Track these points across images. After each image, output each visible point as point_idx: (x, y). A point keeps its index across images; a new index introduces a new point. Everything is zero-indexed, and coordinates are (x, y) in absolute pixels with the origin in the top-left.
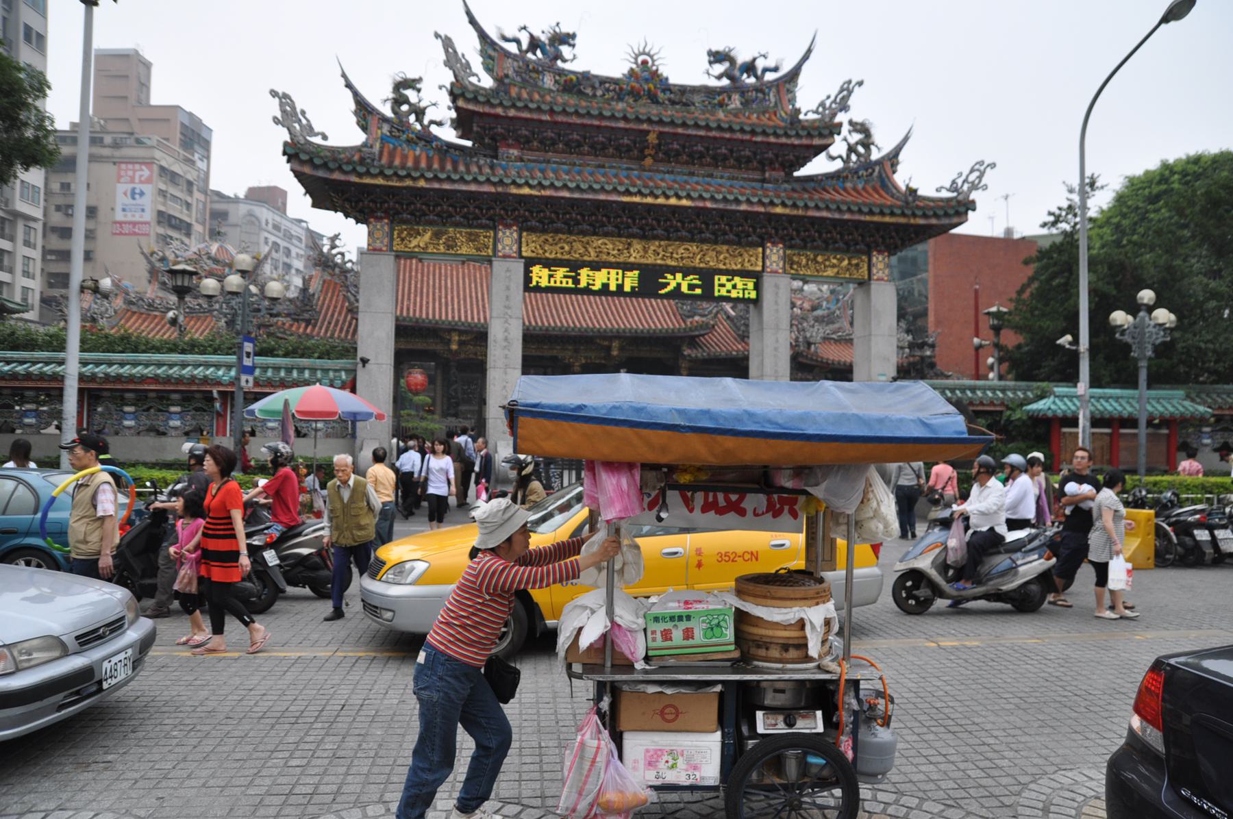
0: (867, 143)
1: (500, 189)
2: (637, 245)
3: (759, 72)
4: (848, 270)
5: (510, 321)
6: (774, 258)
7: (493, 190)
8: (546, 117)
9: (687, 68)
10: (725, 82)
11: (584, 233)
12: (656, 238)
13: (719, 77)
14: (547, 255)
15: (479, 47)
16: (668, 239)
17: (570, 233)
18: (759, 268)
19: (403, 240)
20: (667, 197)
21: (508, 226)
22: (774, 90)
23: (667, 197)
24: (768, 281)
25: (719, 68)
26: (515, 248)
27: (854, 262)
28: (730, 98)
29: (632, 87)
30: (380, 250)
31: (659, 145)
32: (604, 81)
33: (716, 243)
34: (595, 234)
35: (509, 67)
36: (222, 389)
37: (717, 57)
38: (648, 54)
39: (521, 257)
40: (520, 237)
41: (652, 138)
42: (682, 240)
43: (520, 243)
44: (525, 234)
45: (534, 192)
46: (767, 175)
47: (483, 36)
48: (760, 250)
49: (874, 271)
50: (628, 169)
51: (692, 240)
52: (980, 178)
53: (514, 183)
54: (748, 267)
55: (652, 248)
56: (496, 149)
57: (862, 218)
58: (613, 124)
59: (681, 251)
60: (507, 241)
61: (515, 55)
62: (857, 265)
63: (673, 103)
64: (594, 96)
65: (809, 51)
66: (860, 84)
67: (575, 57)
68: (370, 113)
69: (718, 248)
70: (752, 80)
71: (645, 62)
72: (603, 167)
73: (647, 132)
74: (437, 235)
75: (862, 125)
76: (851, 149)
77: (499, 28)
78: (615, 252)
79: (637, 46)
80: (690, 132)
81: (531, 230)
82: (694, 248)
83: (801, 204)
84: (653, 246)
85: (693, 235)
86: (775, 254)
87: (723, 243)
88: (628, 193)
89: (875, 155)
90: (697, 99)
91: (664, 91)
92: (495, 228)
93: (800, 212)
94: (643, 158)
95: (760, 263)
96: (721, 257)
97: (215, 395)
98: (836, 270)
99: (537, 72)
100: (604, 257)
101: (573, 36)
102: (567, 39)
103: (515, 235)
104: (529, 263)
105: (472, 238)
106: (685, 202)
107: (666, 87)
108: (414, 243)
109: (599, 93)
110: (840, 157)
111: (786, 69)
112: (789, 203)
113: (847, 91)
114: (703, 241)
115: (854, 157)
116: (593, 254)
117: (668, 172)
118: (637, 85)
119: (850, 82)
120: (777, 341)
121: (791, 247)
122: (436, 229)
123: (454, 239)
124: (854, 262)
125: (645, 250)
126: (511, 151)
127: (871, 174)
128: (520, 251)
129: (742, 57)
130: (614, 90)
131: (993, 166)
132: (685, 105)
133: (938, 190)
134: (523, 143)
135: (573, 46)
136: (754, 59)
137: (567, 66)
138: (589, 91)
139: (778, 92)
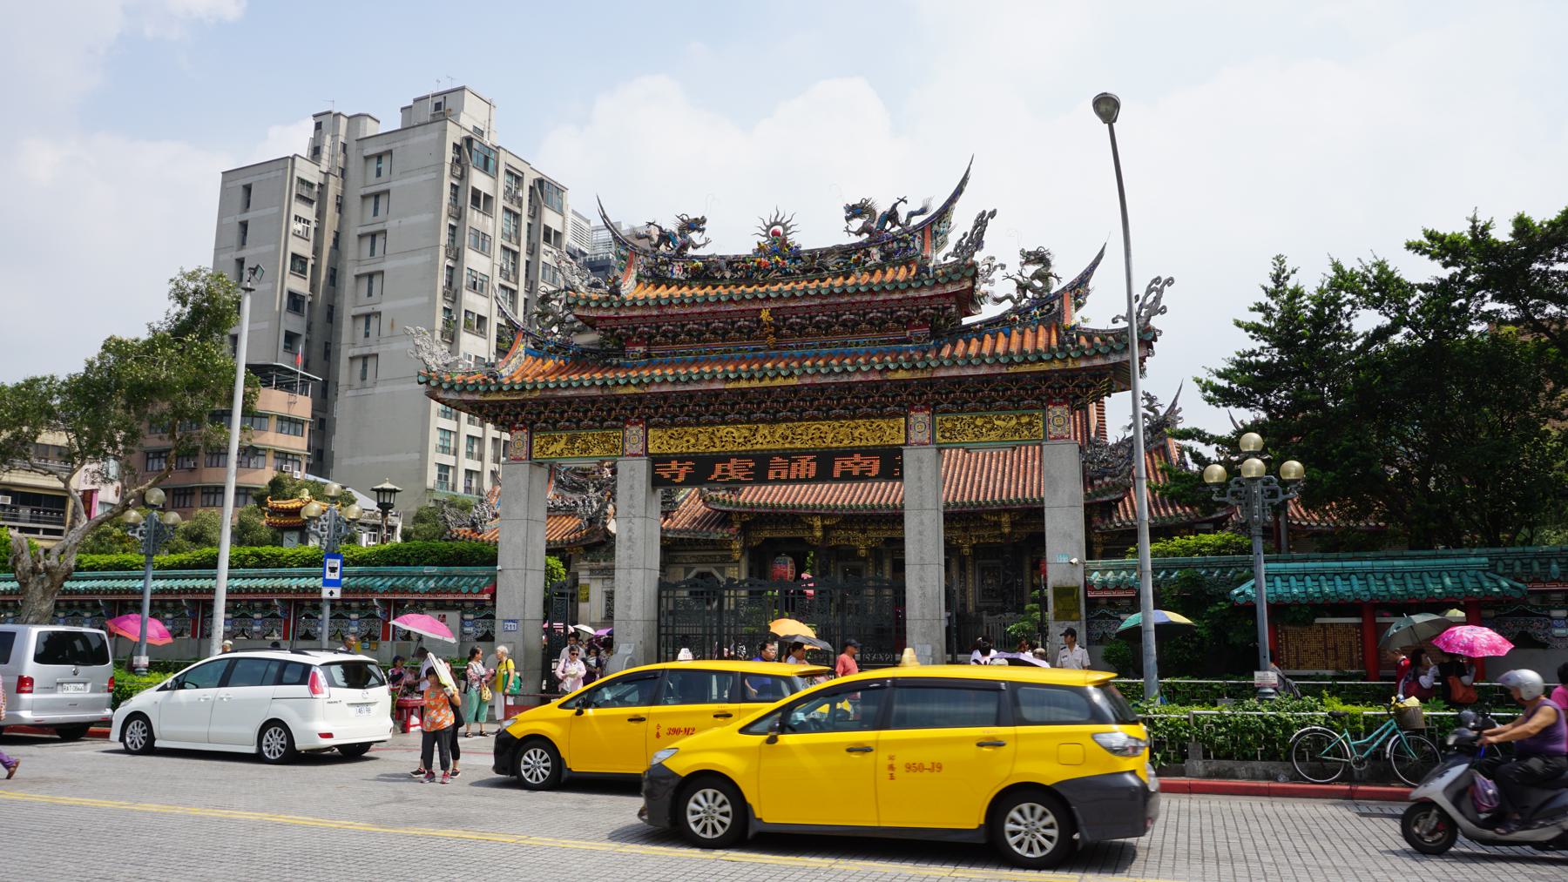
0: (1043, 277)
2: (764, 429)
3: (902, 218)
4: (1017, 431)
5: (636, 520)
9: (821, 229)
10: (866, 236)
13: (859, 233)
21: (636, 424)
24: (909, 456)
25: (857, 223)
27: (1025, 420)
28: (868, 254)
32: (731, 262)
37: (855, 211)
39: (647, 454)
42: (814, 419)
52: (1157, 300)
56: (623, 349)
59: (811, 431)
62: (1030, 423)
64: (723, 278)
66: (993, 214)
67: (707, 241)
70: (897, 228)
71: (775, 233)
74: (572, 440)
75: (1036, 253)
76: (1022, 288)
81: (658, 426)
84: (781, 429)
89: (1056, 287)
90: (831, 262)
91: (794, 261)
92: (623, 428)
100: (729, 447)
101: (703, 221)
102: (696, 225)
107: (796, 255)
109: (728, 275)
110: (1009, 297)
111: (935, 207)
113: (981, 222)
114: (838, 418)
115: (1029, 294)
117: (797, 347)
120: (922, 523)
124: (1025, 420)
125: (772, 434)
129: (882, 207)
131: (1170, 281)
133: (1114, 321)
134: (648, 340)
137: (700, 252)
138: (718, 275)
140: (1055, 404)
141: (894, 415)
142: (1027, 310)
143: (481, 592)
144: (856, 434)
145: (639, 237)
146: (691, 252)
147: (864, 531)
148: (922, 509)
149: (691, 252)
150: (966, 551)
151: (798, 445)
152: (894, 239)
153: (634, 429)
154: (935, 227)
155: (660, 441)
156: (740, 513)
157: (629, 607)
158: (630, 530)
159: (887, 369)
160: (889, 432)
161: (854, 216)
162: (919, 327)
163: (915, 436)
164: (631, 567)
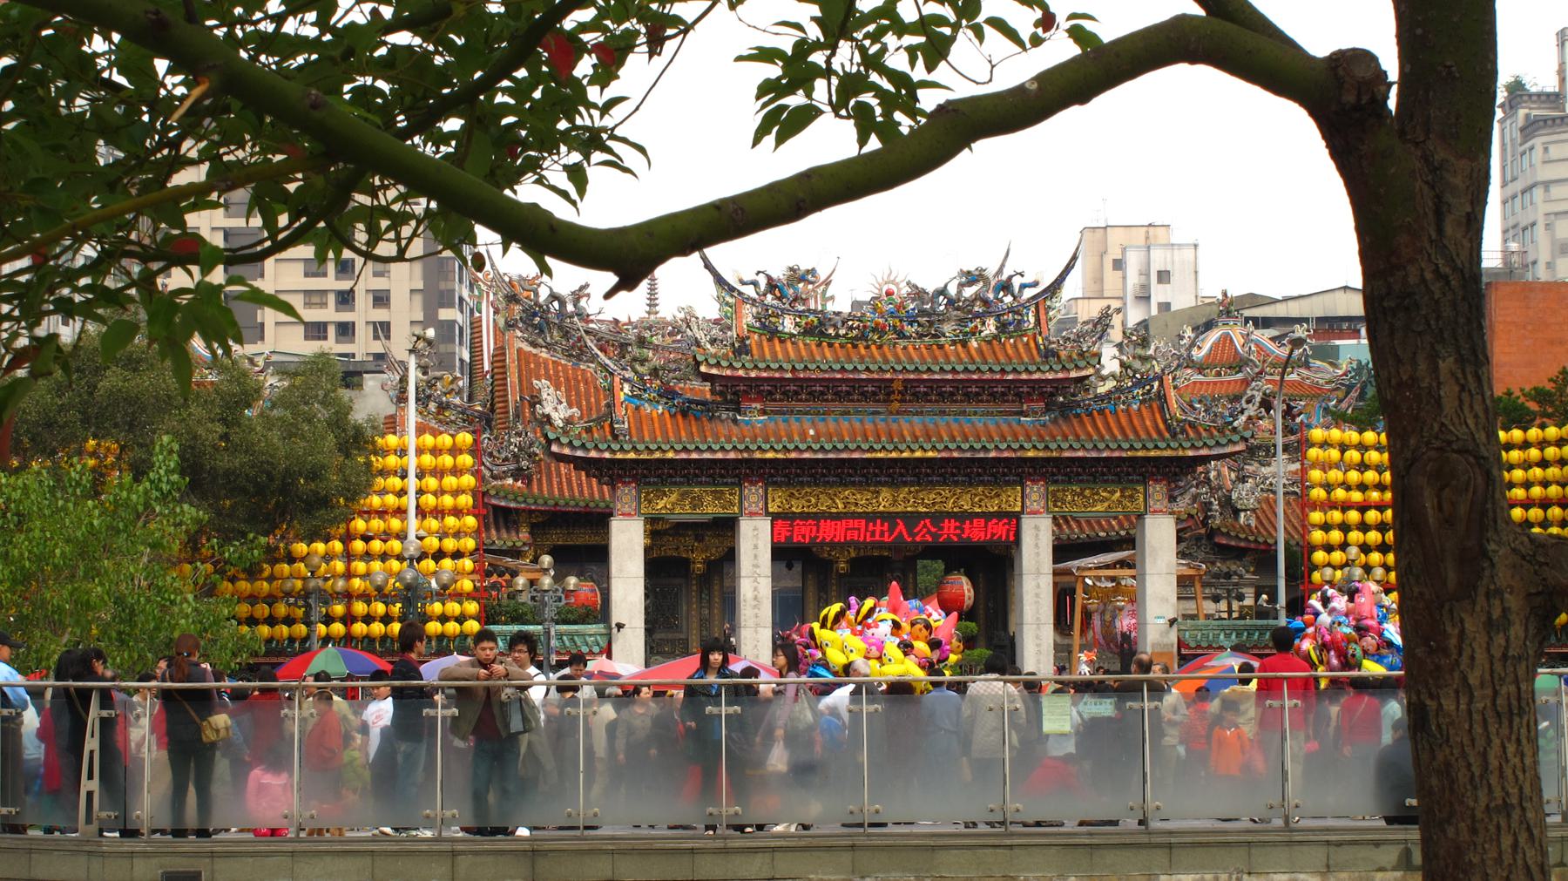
1: (746, 455)
3: (1016, 290)
6: (1035, 497)
8: (789, 375)
11: (831, 484)
12: (905, 484)
16: (919, 484)
17: (817, 485)
20: (913, 451)
21: (753, 483)
23: (913, 451)
24: (1027, 524)
26: (761, 505)
29: (877, 324)
33: (971, 485)
35: (748, 315)
38: (893, 282)
39: (768, 514)
41: (898, 386)
45: (780, 456)
47: (720, 281)
51: (945, 483)
53: (759, 448)
60: (753, 498)
62: (1131, 496)
63: (921, 336)
64: (837, 336)
65: (1074, 258)
70: (1008, 299)
72: (848, 413)
73: (892, 380)
74: (683, 496)
81: (777, 485)
83: (1053, 446)
86: (1035, 493)
88: (872, 449)
92: (740, 485)
93: (1055, 454)
99: (777, 316)
104: (775, 517)
105: (718, 496)
106: (930, 454)
112: (1041, 446)
114: (956, 483)
120: (1038, 586)
121: (1056, 482)
123: (700, 499)
132: (935, 336)
134: (762, 396)
136: (1010, 278)
138: (831, 331)
140: (1156, 481)
141: (1008, 483)
142: (1130, 390)
145: (743, 283)
147: (699, 539)
148: (1038, 573)
151: (922, 509)
152: (1011, 310)
156: (531, 512)
159: (1022, 447)
160: (1010, 500)
164: (757, 625)
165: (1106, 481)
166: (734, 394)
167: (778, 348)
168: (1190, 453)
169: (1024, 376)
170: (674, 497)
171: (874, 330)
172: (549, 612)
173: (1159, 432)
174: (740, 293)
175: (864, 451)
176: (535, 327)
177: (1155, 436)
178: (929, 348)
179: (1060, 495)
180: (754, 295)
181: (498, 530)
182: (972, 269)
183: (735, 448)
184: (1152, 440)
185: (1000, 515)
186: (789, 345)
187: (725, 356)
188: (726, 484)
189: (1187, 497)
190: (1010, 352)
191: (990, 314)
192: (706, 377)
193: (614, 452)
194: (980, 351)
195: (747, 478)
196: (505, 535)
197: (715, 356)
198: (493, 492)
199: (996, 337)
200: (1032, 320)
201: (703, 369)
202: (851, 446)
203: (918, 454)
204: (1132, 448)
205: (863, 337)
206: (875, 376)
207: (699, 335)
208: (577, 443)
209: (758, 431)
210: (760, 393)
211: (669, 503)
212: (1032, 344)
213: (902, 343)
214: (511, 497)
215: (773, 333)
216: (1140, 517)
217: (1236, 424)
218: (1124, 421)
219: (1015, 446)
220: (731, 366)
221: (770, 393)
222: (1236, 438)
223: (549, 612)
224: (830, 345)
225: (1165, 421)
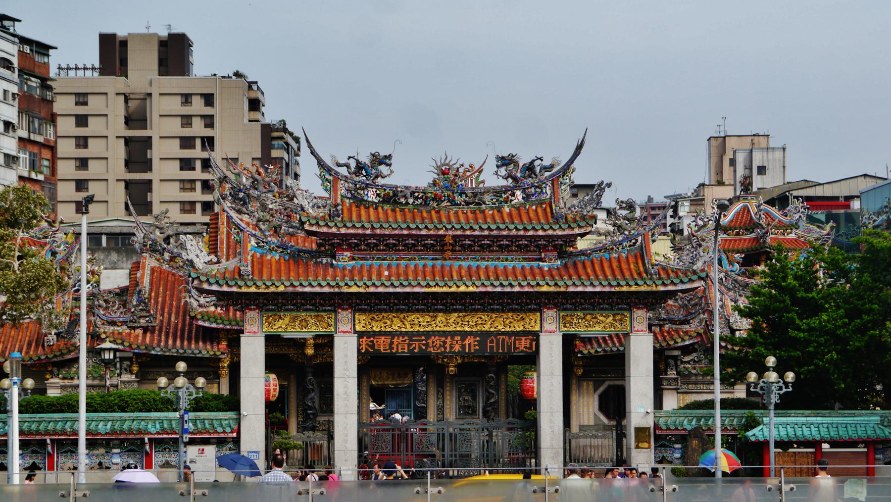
1: (337, 290)
2: (441, 317)
7: (332, 290)
8: (368, 232)
11: (402, 311)
12: (455, 311)
14: (374, 329)
15: (318, 174)
16: (466, 311)
17: (391, 311)
18: (537, 328)
19: (269, 324)
20: (458, 287)
21: (347, 309)
22: (549, 183)
24: (544, 339)
28: (513, 195)
29: (436, 195)
30: (254, 332)
31: (455, 241)
33: (503, 311)
34: (408, 311)
35: (342, 188)
36: (150, 436)
39: (355, 332)
40: (354, 318)
41: (449, 240)
43: (354, 321)
44: (357, 316)
45: (361, 290)
46: (543, 255)
47: (321, 164)
48: (538, 314)
49: (635, 324)
50: (433, 259)
51: (484, 311)
54: (529, 328)
55: (452, 320)
57: (613, 290)
58: (418, 233)
59: (475, 319)
61: (346, 177)
62: (621, 320)
63: (468, 204)
64: (407, 203)
65: (579, 148)
66: (609, 185)
67: (392, 172)
68: (241, 230)
69: (505, 316)
73: (445, 236)
74: (293, 319)
75: (626, 204)
77: (332, 156)
78: (425, 323)
79: (439, 158)
80: (477, 233)
81: (363, 311)
82: (485, 317)
83: (561, 283)
85: (484, 307)
87: (509, 311)
88: (428, 286)
90: (487, 198)
91: (460, 195)
92: (335, 311)
93: (562, 289)
94: (443, 251)
95: (539, 325)
96: (508, 322)
97: (147, 441)
98: (602, 325)
99: (363, 189)
100: (417, 328)
101: (389, 157)
103: (350, 316)
104: (361, 335)
108: (278, 324)
109: (411, 201)
114: (493, 311)
116: (409, 327)
118: (439, 192)
119: (602, 183)
120: (552, 385)
122: (295, 313)
124: (618, 318)
126: (345, 253)
127: (634, 244)
128: (354, 328)
129: (523, 160)
130: (422, 197)
135: (390, 165)
136: (533, 161)
138: (403, 200)
139: (553, 184)
140: (639, 309)
141: (530, 310)
143: (232, 432)
144: (508, 322)
145: (339, 165)
146: (380, 181)
148: (552, 376)
149: (380, 181)
150: (452, 369)
151: (467, 329)
153: (345, 313)
154: (561, 180)
155: (363, 322)
157: (346, 441)
158: (346, 386)
159: (538, 284)
160: (532, 323)
161: (503, 165)
162: (551, 251)
163: (547, 326)
164: (347, 413)
165: (603, 309)
166: (330, 245)
167: (363, 212)
168: (662, 288)
169: (541, 233)
170: (287, 320)
171: (434, 199)
172: (184, 404)
173: (640, 274)
174: (337, 173)
175: (422, 287)
176: (241, 199)
177: (636, 276)
178: (473, 212)
179: (569, 319)
180: (346, 174)
181: (197, 342)
182: (506, 155)
183: (328, 284)
184: (633, 279)
185: (526, 333)
186: (371, 210)
187: (323, 218)
188: (325, 311)
189: (697, 320)
190: (532, 215)
191: (517, 187)
192: (310, 233)
193: (240, 287)
194: (510, 214)
195: (340, 306)
196: (209, 347)
197: (315, 218)
198: (199, 317)
199: (521, 204)
200: (549, 192)
201: (307, 227)
202: (413, 283)
203: (463, 289)
204: (619, 285)
205: (426, 204)
206: (432, 232)
207: (305, 203)
208: (212, 280)
209: (350, 273)
210: (349, 245)
211: (286, 326)
212: (548, 210)
213: (455, 209)
214: (212, 320)
215: (360, 202)
216: (627, 335)
217: (695, 268)
218: (615, 264)
219: (533, 283)
220: (326, 225)
221: (357, 245)
222: (694, 277)
223: (184, 404)
224: (402, 210)
225: (644, 264)
